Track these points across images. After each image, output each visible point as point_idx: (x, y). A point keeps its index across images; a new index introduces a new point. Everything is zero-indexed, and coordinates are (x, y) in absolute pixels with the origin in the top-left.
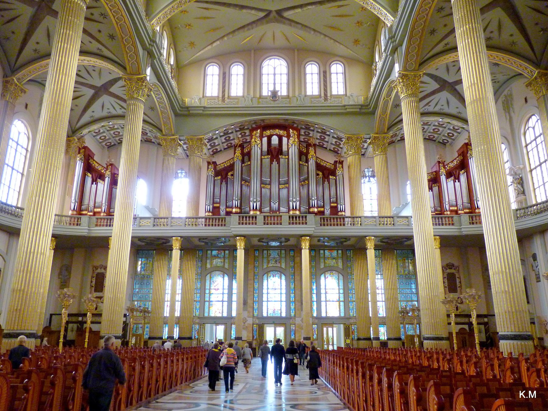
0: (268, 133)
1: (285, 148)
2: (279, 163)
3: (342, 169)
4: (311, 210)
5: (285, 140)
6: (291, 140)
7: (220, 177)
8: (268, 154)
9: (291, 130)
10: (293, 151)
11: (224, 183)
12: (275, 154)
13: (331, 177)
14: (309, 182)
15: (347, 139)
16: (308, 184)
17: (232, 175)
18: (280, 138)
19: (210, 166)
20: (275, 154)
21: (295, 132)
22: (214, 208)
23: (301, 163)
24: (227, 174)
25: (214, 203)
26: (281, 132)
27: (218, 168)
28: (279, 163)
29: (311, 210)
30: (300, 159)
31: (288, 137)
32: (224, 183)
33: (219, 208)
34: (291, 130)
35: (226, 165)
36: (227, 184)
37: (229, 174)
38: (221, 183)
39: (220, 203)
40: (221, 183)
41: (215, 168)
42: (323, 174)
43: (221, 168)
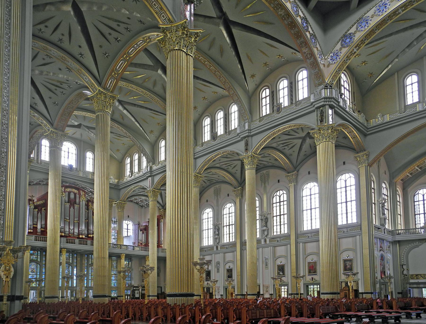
0: (69, 190)
1: (77, 201)
2: (74, 208)
4: (90, 236)
5: (77, 196)
7: (37, 210)
8: (68, 202)
10: (83, 203)
11: (39, 214)
12: (72, 203)
16: (88, 222)
17: (44, 210)
18: (75, 194)
20: (72, 203)
22: (33, 227)
24: (41, 209)
25: (33, 224)
26: (76, 191)
28: (74, 208)
29: (90, 236)
32: (39, 214)
33: (36, 228)
36: (41, 214)
37: (43, 209)
38: (38, 214)
39: (37, 225)
40: (38, 214)
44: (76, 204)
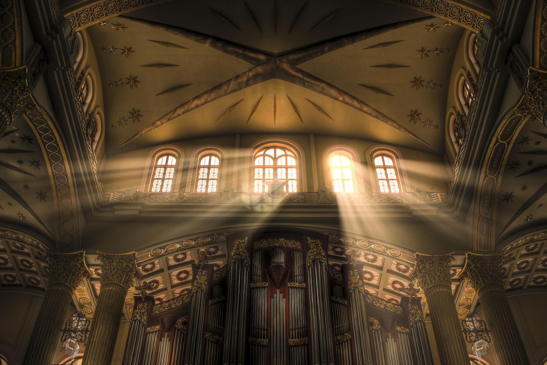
3: (419, 311)
6: (310, 255)
7: (157, 327)
9: (310, 240)
13: (398, 328)
14: (352, 334)
15: (421, 261)
19: (140, 306)
21: (319, 242)
23: (333, 298)
27: (156, 311)
30: (331, 293)
31: (305, 249)
34: (310, 240)
35: (173, 306)
37: (180, 321)
41: (150, 311)
42: (381, 322)
43: (162, 310)
44: (292, 279)
